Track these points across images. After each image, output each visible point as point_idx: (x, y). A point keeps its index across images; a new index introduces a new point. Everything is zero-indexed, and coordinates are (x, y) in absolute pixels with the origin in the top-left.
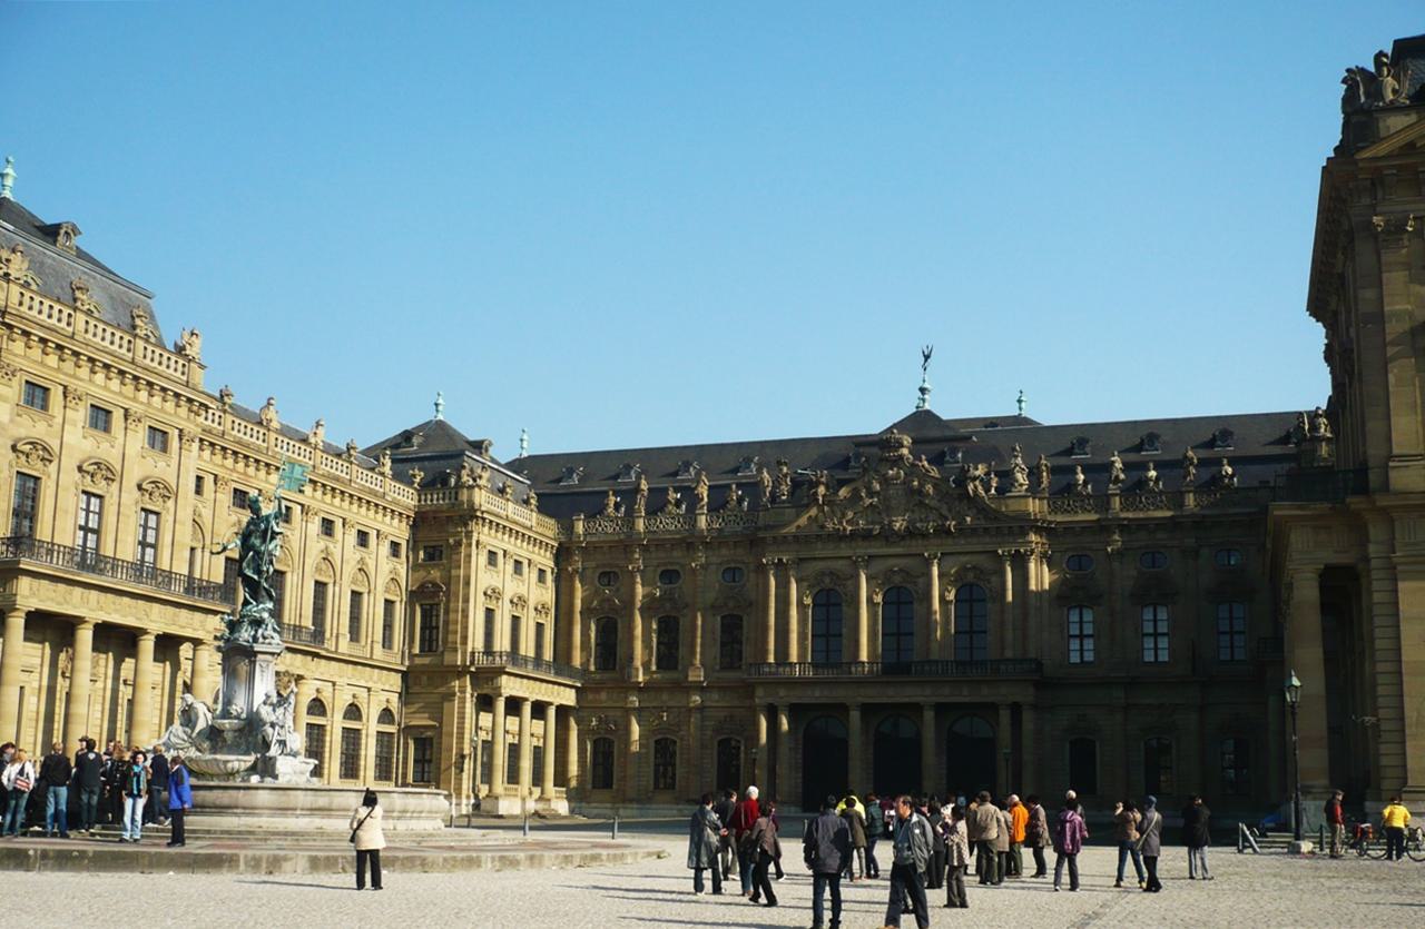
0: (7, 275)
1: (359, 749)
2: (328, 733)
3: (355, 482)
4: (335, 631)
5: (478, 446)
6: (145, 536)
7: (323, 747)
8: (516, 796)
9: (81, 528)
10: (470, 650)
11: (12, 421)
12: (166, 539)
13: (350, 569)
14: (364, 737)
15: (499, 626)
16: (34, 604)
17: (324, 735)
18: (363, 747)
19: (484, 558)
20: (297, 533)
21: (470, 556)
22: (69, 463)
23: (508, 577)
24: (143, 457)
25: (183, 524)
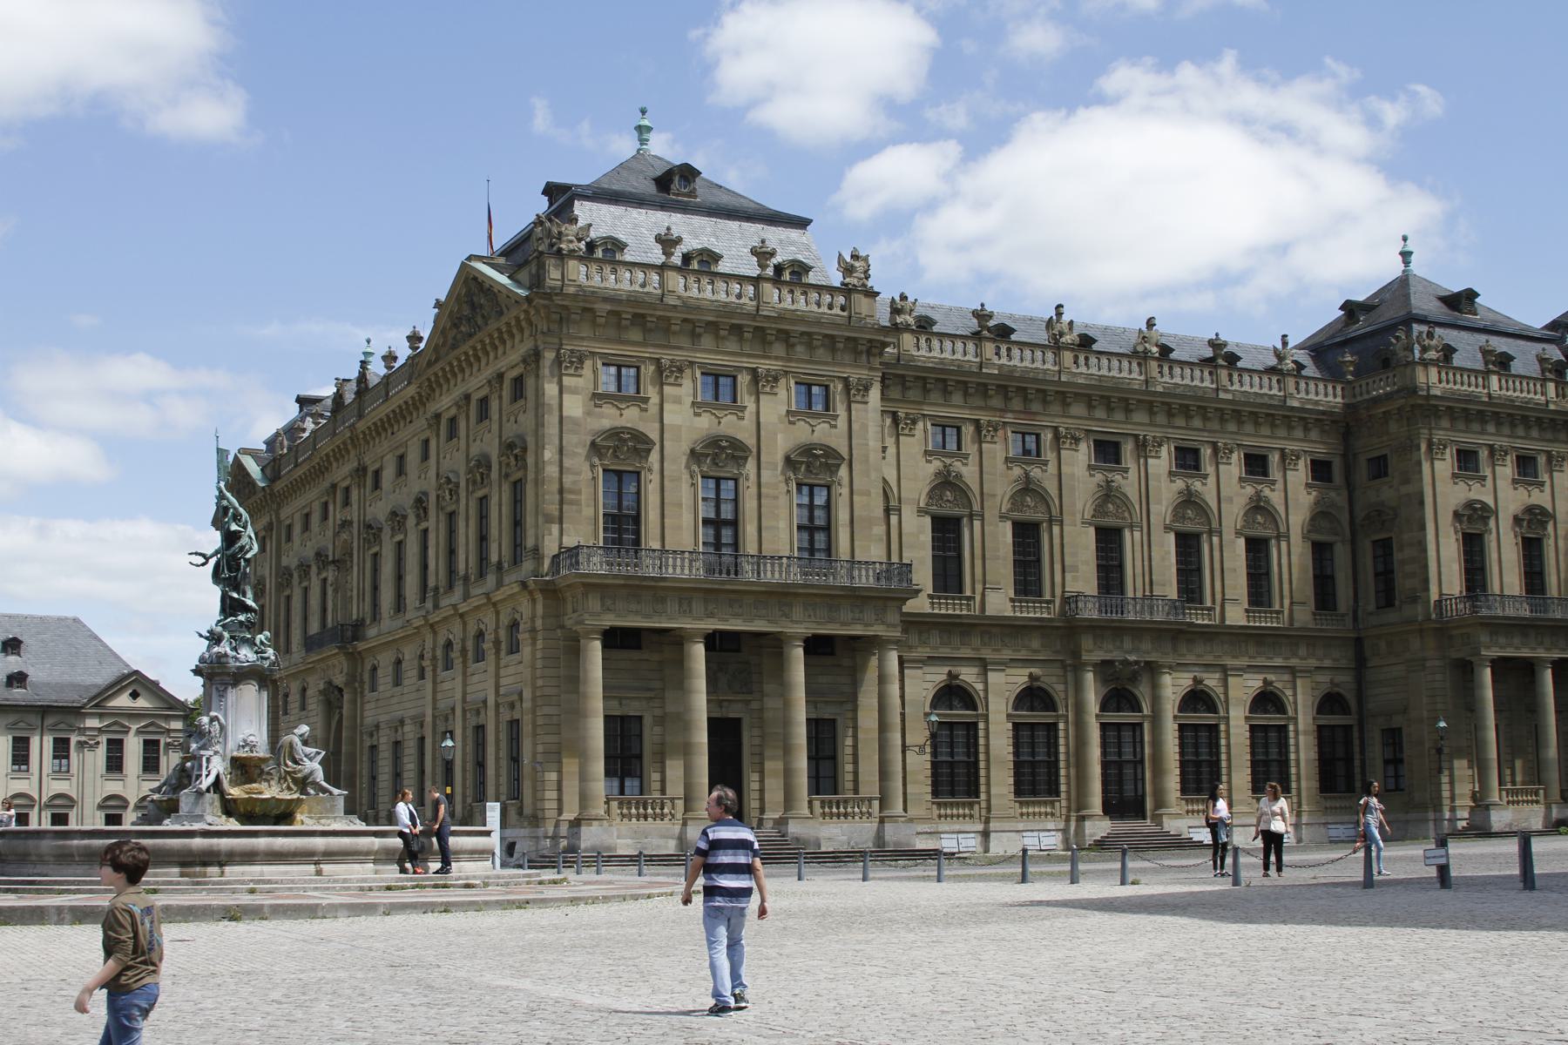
0: (560, 250)
1: (1287, 753)
2: (1223, 735)
3: (1227, 391)
4: (1218, 597)
5: (1462, 301)
6: (811, 518)
7: (1218, 754)
8: (1537, 802)
9: (706, 522)
10: (1434, 596)
11: (588, 413)
12: (842, 515)
13: (1233, 513)
14: (1292, 734)
15: (1494, 556)
16: (610, 621)
17: (1218, 738)
18: (1292, 749)
19: (1445, 466)
20: (1133, 474)
21: (1419, 463)
22: (677, 449)
23: (1504, 485)
24: (791, 423)
25: (868, 494)
